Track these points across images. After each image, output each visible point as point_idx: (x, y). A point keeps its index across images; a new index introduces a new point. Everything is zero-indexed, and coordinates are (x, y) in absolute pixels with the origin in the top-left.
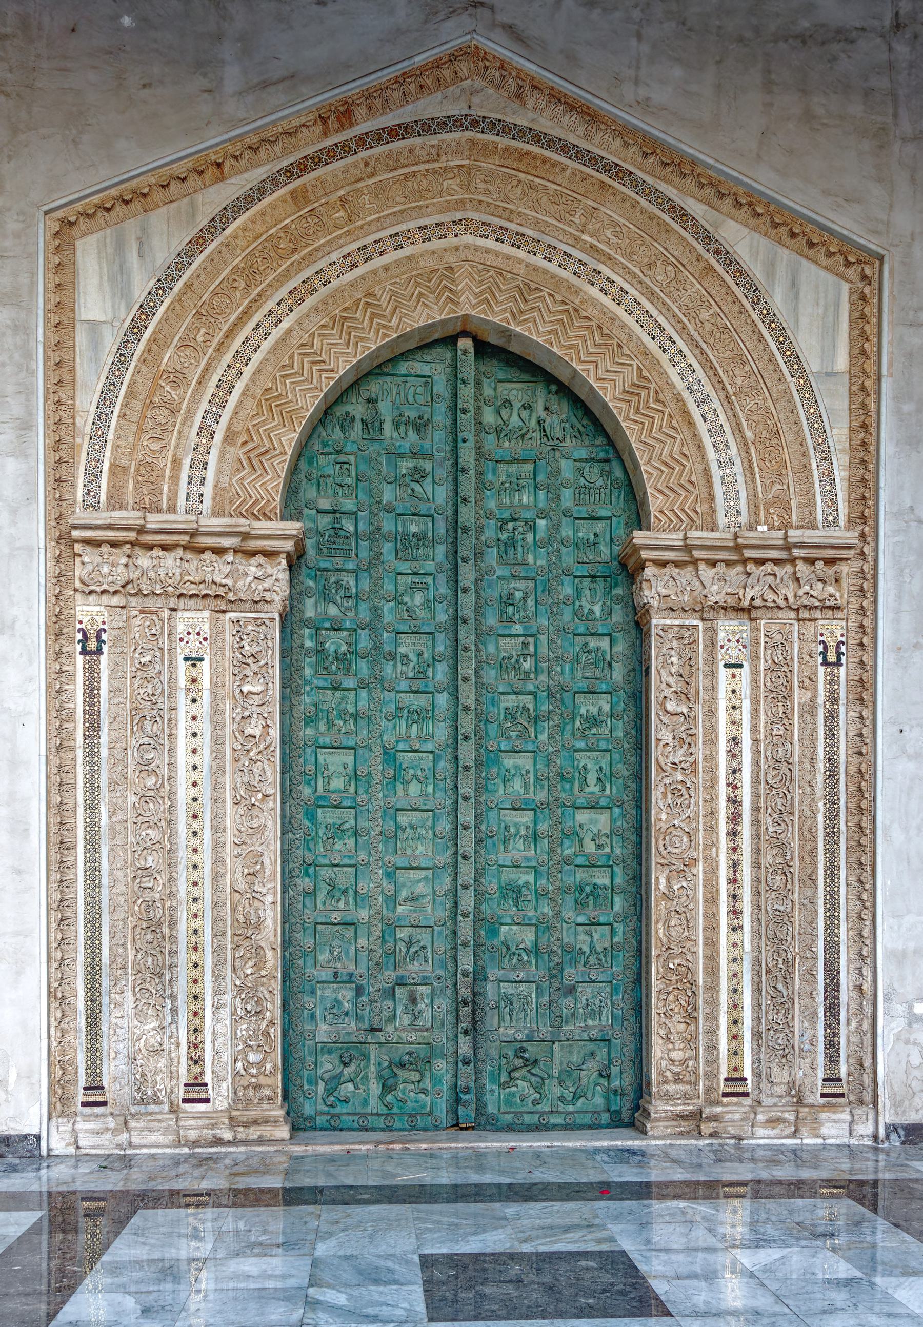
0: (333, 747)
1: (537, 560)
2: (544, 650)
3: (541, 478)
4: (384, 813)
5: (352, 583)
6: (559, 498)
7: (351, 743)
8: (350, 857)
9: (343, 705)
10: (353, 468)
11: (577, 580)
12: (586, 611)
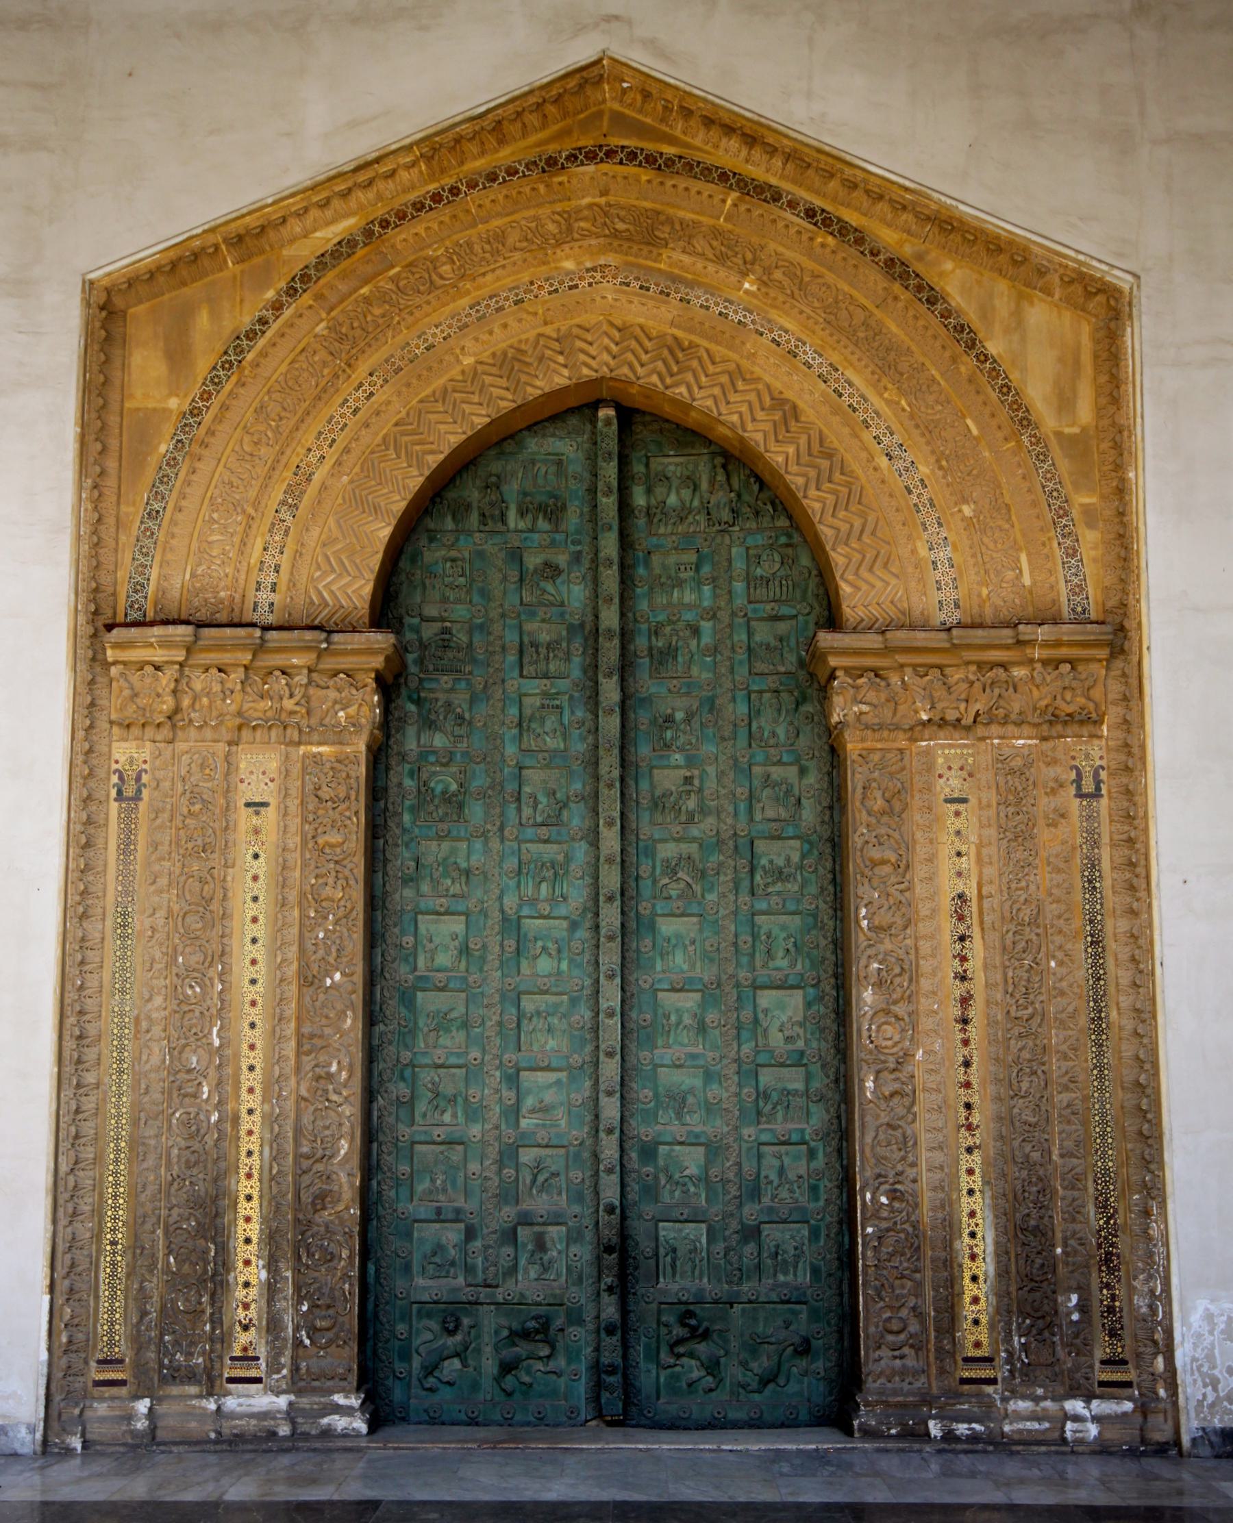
0: (438, 913)
2: (711, 784)
3: (706, 569)
4: (503, 997)
5: (465, 706)
6: (730, 592)
7: (461, 908)
8: (458, 1055)
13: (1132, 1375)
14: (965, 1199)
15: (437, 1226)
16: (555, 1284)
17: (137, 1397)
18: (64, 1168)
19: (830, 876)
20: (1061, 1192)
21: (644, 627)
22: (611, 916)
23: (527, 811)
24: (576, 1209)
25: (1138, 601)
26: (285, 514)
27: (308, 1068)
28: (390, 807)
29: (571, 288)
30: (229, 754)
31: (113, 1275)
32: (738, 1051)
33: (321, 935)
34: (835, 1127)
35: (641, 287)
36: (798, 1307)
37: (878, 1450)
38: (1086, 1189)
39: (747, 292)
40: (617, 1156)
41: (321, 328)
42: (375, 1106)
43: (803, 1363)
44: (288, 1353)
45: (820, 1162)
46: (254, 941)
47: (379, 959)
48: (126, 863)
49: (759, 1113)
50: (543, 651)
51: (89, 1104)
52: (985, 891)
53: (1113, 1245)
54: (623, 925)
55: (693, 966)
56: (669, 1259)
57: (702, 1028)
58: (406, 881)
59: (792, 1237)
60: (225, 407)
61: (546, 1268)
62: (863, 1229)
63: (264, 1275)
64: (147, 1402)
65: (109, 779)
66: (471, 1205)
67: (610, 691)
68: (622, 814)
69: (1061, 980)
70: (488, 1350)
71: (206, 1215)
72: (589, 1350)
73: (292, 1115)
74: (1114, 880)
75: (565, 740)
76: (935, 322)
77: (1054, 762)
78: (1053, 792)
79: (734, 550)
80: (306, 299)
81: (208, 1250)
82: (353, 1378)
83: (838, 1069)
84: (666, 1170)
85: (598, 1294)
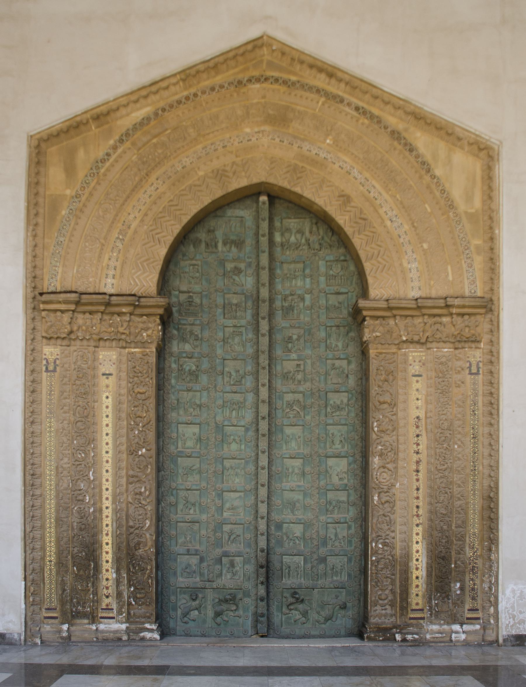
0: (187, 424)
1: (305, 318)
2: (309, 368)
3: (307, 271)
5: (199, 332)
6: (318, 281)
7: (198, 421)
9: (193, 400)
10: (200, 268)
11: (328, 328)
12: (333, 346)
13: (480, 615)
14: (415, 545)
15: (188, 556)
16: (238, 581)
17: (63, 623)
18: (28, 530)
19: (360, 409)
20: (455, 542)
21: (280, 297)
22: (264, 426)
23: (226, 379)
24: (248, 550)
25: (499, 288)
26: (119, 244)
27: (131, 490)
28: (166, 376)
29: (248, 141)
30: (94, 352)
31: (50, 574)
32: (318, 485)
33: (136, 432)
34: (360, 516)
35: (280, 141)
36: (341, 590)
37: (374, 646)
38: (465, 541)
39: (328, 144)
40: (266, 528)
41: (134, 158)
42: (160, 506)
43: (343, 612)
44: (126, 607)
45: (352, 531)
46: (107, 434)
47: (161, 443)
48: (50, 400)
49: (327, 510)
50: (234, 307)
51: (38, 503)
52: (428, 415)
53: (475, 563)
54: (269, 429)
55: (299, 448)
56: (287, 571)
57: (304, 474)
58: (174, 409)
59: (340, 562)
60: (91, 194)
61: (234, 575)
62: (371, 558)
63: (114, 575)
64: (67, 625)
65: (42, 362)
66: (203, 548)
67: (264, 326)
68: (269, 380)
69: (459, 454)
70: (209, 607)
71: (89, 551)
72: (253, 607)
73: (125, 509)
74: (483, 410)
75: (243, 347)
76: (412, 160)
77: (459, 359)
78: (459, 372)
79: (320, 262)
80: (128, 144)
81: (90, 565)
82: (153, 618)
83: (361, 492)
84: (286, 534)
85: (257, 585)
